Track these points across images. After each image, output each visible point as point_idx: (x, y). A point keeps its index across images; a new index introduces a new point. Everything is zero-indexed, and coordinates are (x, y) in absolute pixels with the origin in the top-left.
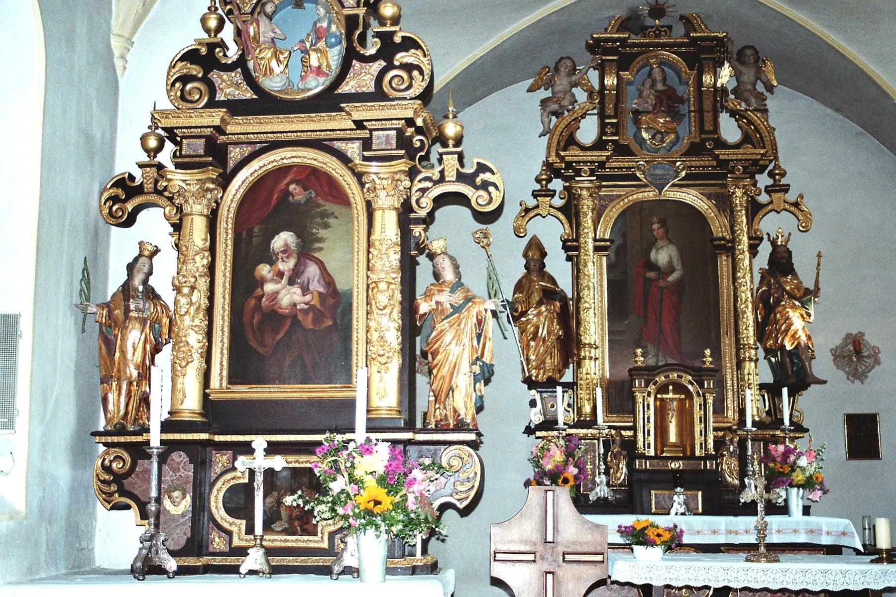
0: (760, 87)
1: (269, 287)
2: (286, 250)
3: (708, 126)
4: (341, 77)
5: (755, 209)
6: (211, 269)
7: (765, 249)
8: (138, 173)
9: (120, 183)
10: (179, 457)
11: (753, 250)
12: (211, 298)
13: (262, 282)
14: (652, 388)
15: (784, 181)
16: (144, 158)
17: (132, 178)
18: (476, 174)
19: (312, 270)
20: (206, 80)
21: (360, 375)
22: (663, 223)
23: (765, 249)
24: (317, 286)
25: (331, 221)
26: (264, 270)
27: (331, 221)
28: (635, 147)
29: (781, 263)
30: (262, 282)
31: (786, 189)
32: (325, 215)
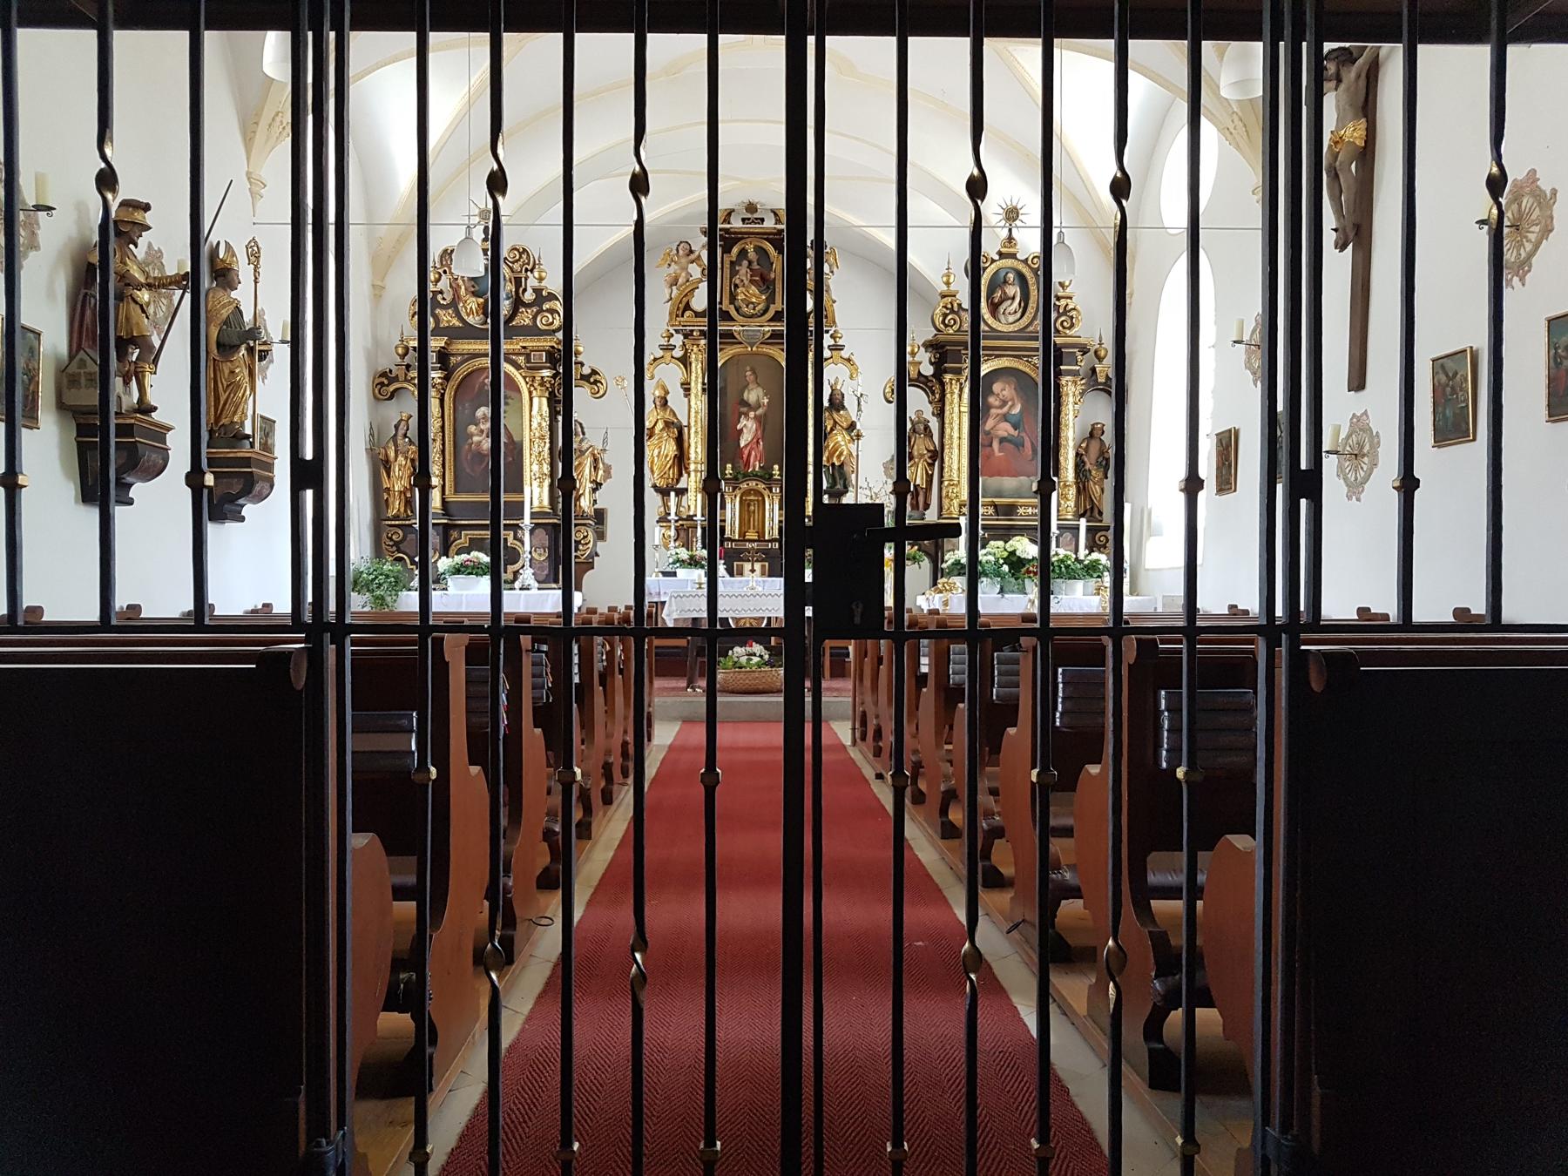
1: (476, 439)
2: (485, 417)
6: (443, 427)
8: (394, 369)
9: (384, 375)
13: (472, 435)
14: (738, 493)
15: (840, 342)
16: (399, 360)
18: (590, 376)
21: (527, 489)
22: (754, 372)
26: (472, 428)
28: (733, 313)
30: (472, 435)
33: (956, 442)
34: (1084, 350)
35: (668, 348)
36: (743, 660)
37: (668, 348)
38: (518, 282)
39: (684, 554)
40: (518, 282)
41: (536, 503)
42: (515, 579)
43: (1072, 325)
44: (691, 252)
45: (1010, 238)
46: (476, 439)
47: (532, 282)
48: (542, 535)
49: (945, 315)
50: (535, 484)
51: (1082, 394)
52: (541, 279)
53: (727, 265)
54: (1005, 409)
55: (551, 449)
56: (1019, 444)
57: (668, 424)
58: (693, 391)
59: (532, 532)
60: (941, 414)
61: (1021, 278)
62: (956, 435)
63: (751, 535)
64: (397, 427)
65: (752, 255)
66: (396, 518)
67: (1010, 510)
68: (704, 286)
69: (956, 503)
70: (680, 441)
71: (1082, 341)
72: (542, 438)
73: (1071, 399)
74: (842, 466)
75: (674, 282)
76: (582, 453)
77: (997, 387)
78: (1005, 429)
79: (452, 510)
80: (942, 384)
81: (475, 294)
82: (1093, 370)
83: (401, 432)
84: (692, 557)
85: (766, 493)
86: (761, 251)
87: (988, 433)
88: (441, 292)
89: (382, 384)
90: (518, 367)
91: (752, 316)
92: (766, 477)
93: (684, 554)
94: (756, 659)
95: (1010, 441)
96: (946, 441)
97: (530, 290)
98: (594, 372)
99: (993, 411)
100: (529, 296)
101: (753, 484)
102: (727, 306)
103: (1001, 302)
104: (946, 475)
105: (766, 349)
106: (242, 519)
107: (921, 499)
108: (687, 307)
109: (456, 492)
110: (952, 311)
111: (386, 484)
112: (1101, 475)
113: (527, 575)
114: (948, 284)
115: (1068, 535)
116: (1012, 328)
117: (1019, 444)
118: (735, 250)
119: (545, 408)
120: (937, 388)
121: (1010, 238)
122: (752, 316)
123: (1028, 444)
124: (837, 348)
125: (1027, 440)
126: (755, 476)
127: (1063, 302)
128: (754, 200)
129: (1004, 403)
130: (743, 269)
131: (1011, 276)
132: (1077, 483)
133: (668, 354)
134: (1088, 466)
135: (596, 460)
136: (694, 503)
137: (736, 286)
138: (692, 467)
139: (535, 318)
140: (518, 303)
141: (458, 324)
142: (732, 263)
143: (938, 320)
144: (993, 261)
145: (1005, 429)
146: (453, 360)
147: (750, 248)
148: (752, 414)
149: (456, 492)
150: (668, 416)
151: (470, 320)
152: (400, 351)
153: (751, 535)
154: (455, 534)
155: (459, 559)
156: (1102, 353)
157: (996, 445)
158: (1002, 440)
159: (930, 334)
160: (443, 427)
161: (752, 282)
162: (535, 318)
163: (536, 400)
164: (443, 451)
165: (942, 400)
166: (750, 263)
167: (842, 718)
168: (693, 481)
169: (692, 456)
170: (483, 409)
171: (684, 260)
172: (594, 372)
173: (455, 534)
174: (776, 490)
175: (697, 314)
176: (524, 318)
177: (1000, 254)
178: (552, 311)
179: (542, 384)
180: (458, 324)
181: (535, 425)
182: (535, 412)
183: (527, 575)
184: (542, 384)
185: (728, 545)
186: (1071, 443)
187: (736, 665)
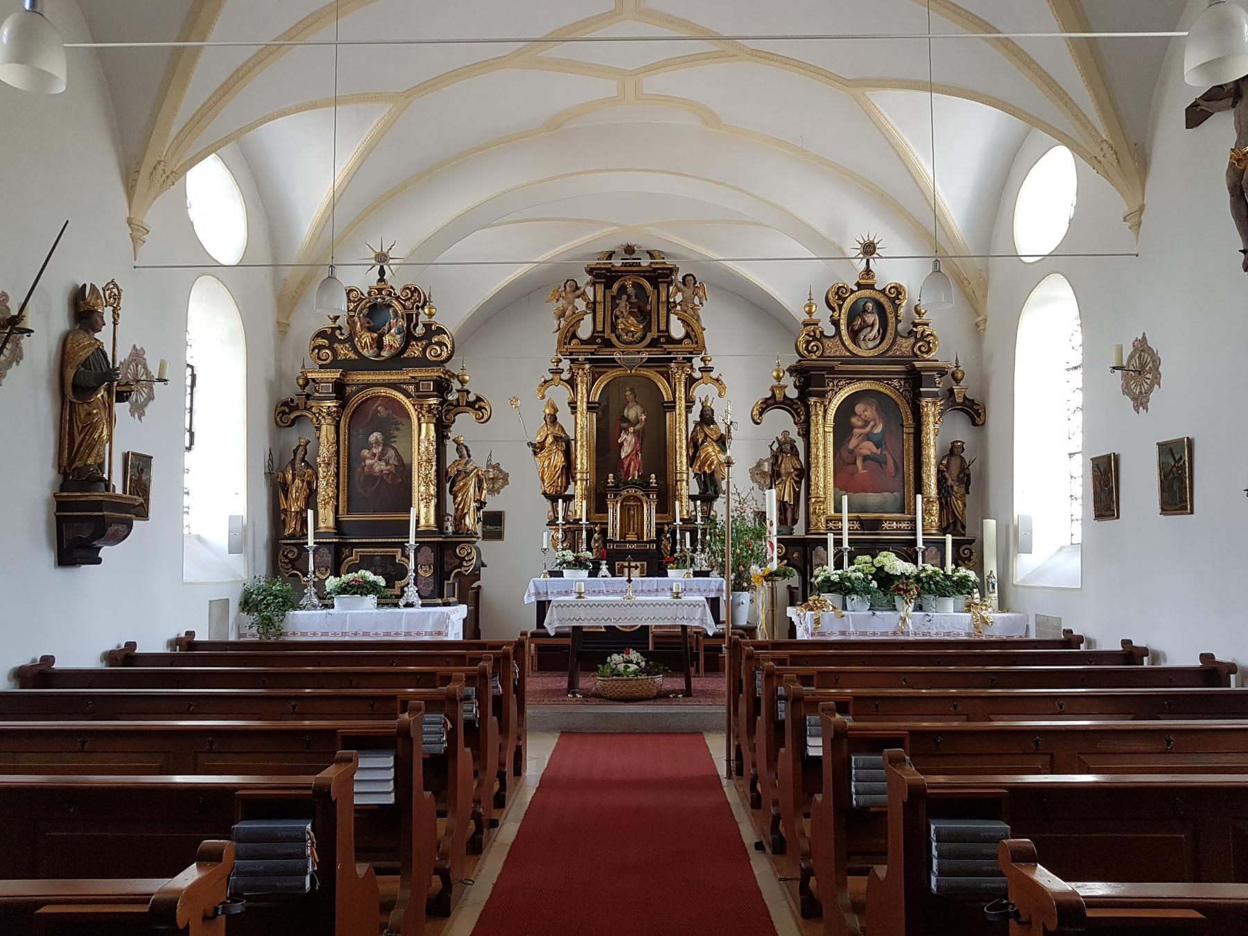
0: (697, 301)
1: (368, 462)
2: (377, 442)
3: (663, 327)
4: (403, 350)
5: (691, 381)
6: (338, 452)
7: (697, 409)
8: (295, 398)
9: (285, 404)
10: (324, 550)
11: (689, 409)
12: (338, 468)
13: (365, 459)
14: (619, 499)
15: (710, 365)
17: (292, 401)
18: (475, 402)
19: (391, 453)
20: (330, 347)
21: (413, 511)
22: (632, 390)
23: (697, 409)
24: (393, 461)
25: (400, 427)
26: (366, 452)
27: (400, 427)
28: (614, 340)
29: (707, 418)
30: (365, 459)
31: (710, 370)
32: (397, 423)
33: (821, 460)
34: (942, 372)
35: (557, 372)
36: (621, 667)
37: (557, 372)
38: (409, 318)
39: (570, 556)
40: (409, 318)
41: (422, 522)
42: (400, 597)
43: (929, 351)
44: (577, 288)
45: (868, 271)
46: (368, 462)
47: (423, 318)
48: (428, 553)
49: (808, 342)
50: (422, 506)
51: (941, 414)
52: (431, 315)
53: (609, 299)
54: (868, 429)
55: (437, 471)
56: (881, 462)
57: (557, 439)
58: (579, 409)
59: (417, 551)
60: (806, 434)
61: (880, 308)
62: (821, 455)
63: (631, 537)
64: (295, 452)
65: (630, 290)
66: (292, 536)
67: (875, 525)
68: (589, 318)
69: (823, 519)
70: (568, 454)
71: (940, 364)
72: (429, 461)
73: (931, 419)
74: (712, 474)
75: (562, 315)
76: (467, 474)
77: (859, 408)
78: (868, 448)
79: (345, 530)
80: (807, 407)
81: (370, 330)
82: (951, 391)
83: (299, 456)
84: (577, 558)
85: (644, 498)
86: (638, 286)
87: (851, 452)
88: (340, 328)
89: (283, 412)
90: (408, 395)
91: (631, 343)
92: (644, 484)
93: (570, 556)
94: (633, 667)
95: (873, 459)
96: (813, 461)
97: (420, 325)
98: (479, 399)
99: (856, 431)
100: (420, 330)
101: (632, 491)
102: (608, 334)
103: (861, 329)
104: (813, 493)
105: (644, 372)
106: (98, 561)
107: (789, 514)
108: (574, 336)
109: (349, 511)
110: (815, 338)
111: (283, 505)
112: (963, 490)
113: (411, 593)
114: (810, 313)
115: (933, 550)
116: (871, 353)
117: (881, 462)
118: (616, 286)
119: (433, 434)
120: (802, 410)
121: (868, 271)
122: (631, 343)
123: (890, 462)
124: (706, 370)
125: (889, 457)
126: (634, 484)
127: (920, 329)
128: (632, 242)
129: (866, 423)
130: (623, 303)
131: (870, 305)
132: (939, 499)
133: (557, 377)
134: (950, 482)
135: (480, 481)
136: (580, 508)
137: (617, 317)
138: (579, 476)
139: (424, 350)
140: (409, 337)
141: (352, 355)
142: (613, 298)
143: (802, 346)
144: (852, 292)
145: (868, 448)
146: (348, 389)
147: (629, 284)
148: (631, 429)
149: (349, 512)
150: (557, 431)
151: (365, 353)
152: (301, 382)
153: (631, 537)
154: (347, 552)
155: (346, 578)
156: (959, 375)
157: (859, 463)
158: (865, 458)
159: (793, 359)
160: (338, 452)
161: (630, 313)
162: (424, 350)
163: (424, 426)
164: (337, 474)
165: (807, 421)
166: (629, 297)
167: (715, 729)
168: (577, 489)
169: (579, 467)
170: (375, 434)
171: (570, 296)
172: (479, 399)
173: (347, 552)
174: (653, 496)
175: (583, 342)
176: (415, 351)
177: (858, 285)
178: (441, 344)
179: (429, 411)
180: (352, 355)
181: (423, 449)
182: (423, 437)
183: (411, 593)
184: (429, 411)
185: (610, 546)
186: (933, 461)
187: (616, 673)
